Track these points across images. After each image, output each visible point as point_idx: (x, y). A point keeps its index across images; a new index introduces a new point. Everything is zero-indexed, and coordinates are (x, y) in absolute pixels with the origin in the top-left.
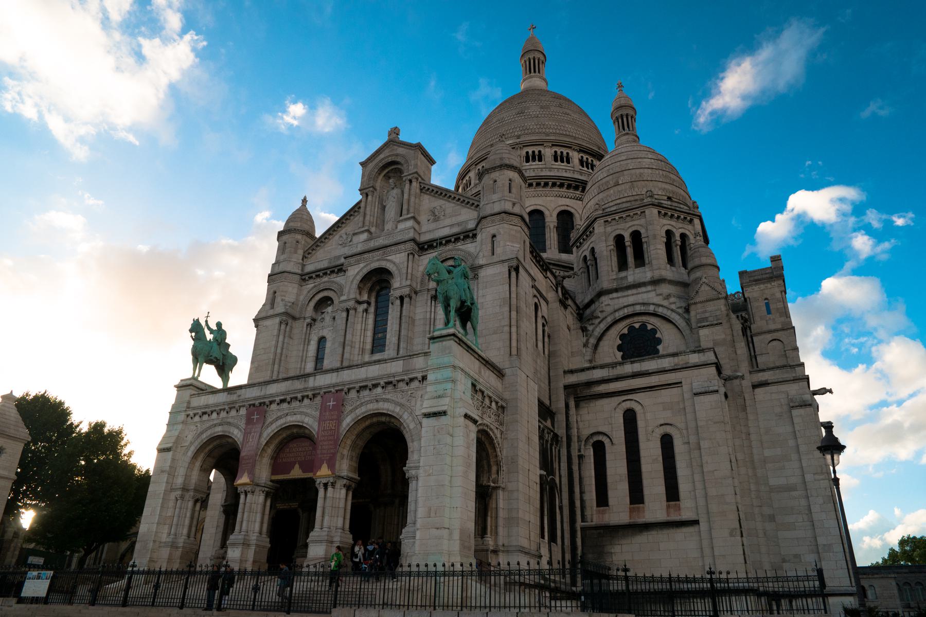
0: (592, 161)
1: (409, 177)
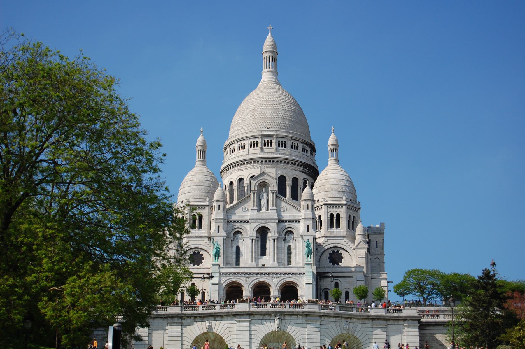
0: (307, 148)
1: (273, 192)
